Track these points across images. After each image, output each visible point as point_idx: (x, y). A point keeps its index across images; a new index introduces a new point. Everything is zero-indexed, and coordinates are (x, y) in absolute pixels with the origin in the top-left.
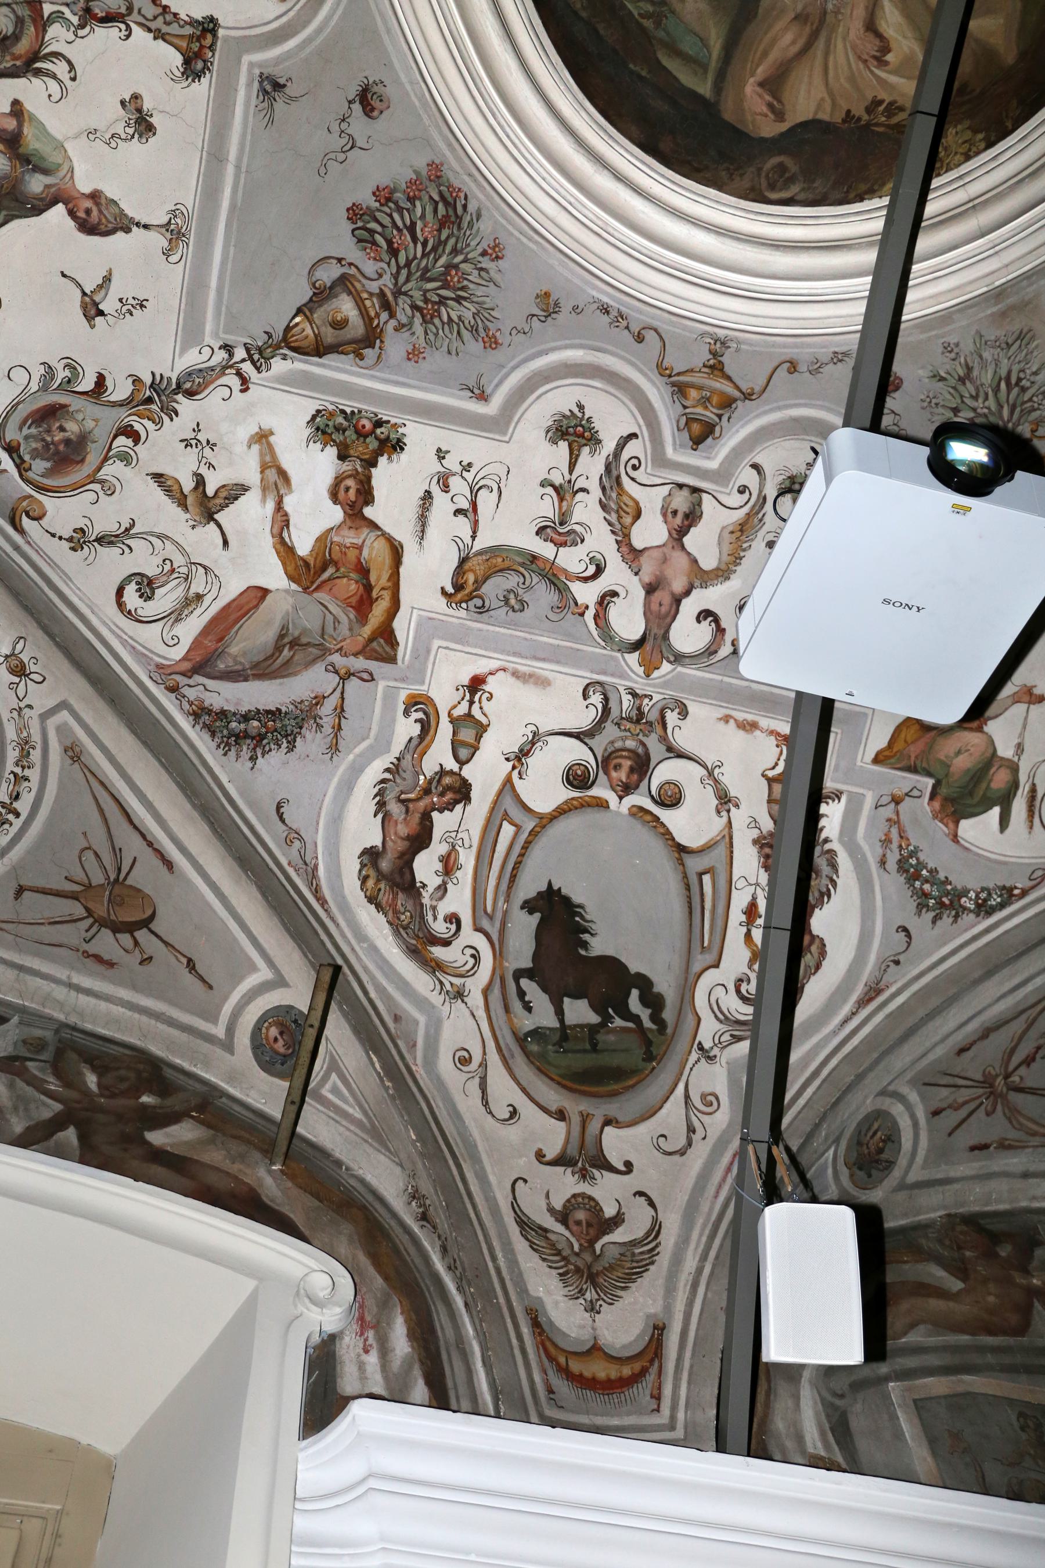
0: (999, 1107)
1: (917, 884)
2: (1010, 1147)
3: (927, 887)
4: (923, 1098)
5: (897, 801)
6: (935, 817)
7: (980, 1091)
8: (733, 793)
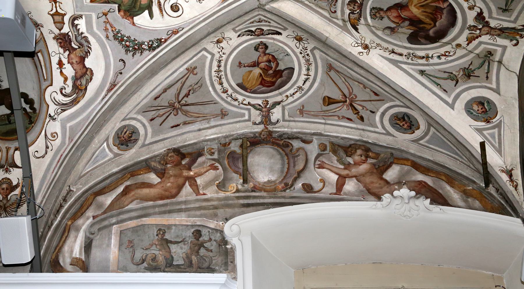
0: (179, 112)
1: (123, 43)
2: (189, 123)
3: (128, 43)
4: (144, 117)
5: (105, 14)
6: (123, 18)
7: (169, 109)
8: (39, 22)
